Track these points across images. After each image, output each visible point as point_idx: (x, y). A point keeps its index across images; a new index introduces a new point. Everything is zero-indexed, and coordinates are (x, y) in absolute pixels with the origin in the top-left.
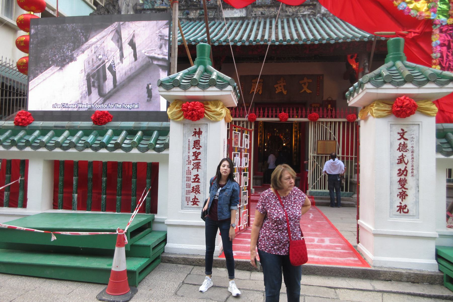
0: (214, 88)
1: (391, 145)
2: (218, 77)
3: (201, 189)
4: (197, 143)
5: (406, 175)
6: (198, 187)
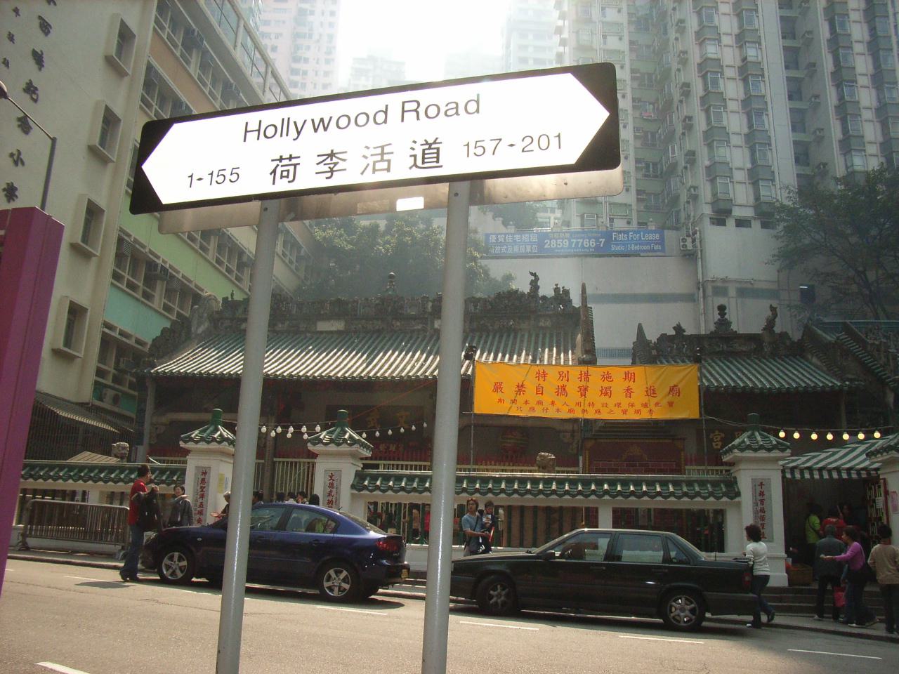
1: (325, 483)
2: (221, 435)
3: (204, 512)
4: (203, 480)
6: (202, 510)
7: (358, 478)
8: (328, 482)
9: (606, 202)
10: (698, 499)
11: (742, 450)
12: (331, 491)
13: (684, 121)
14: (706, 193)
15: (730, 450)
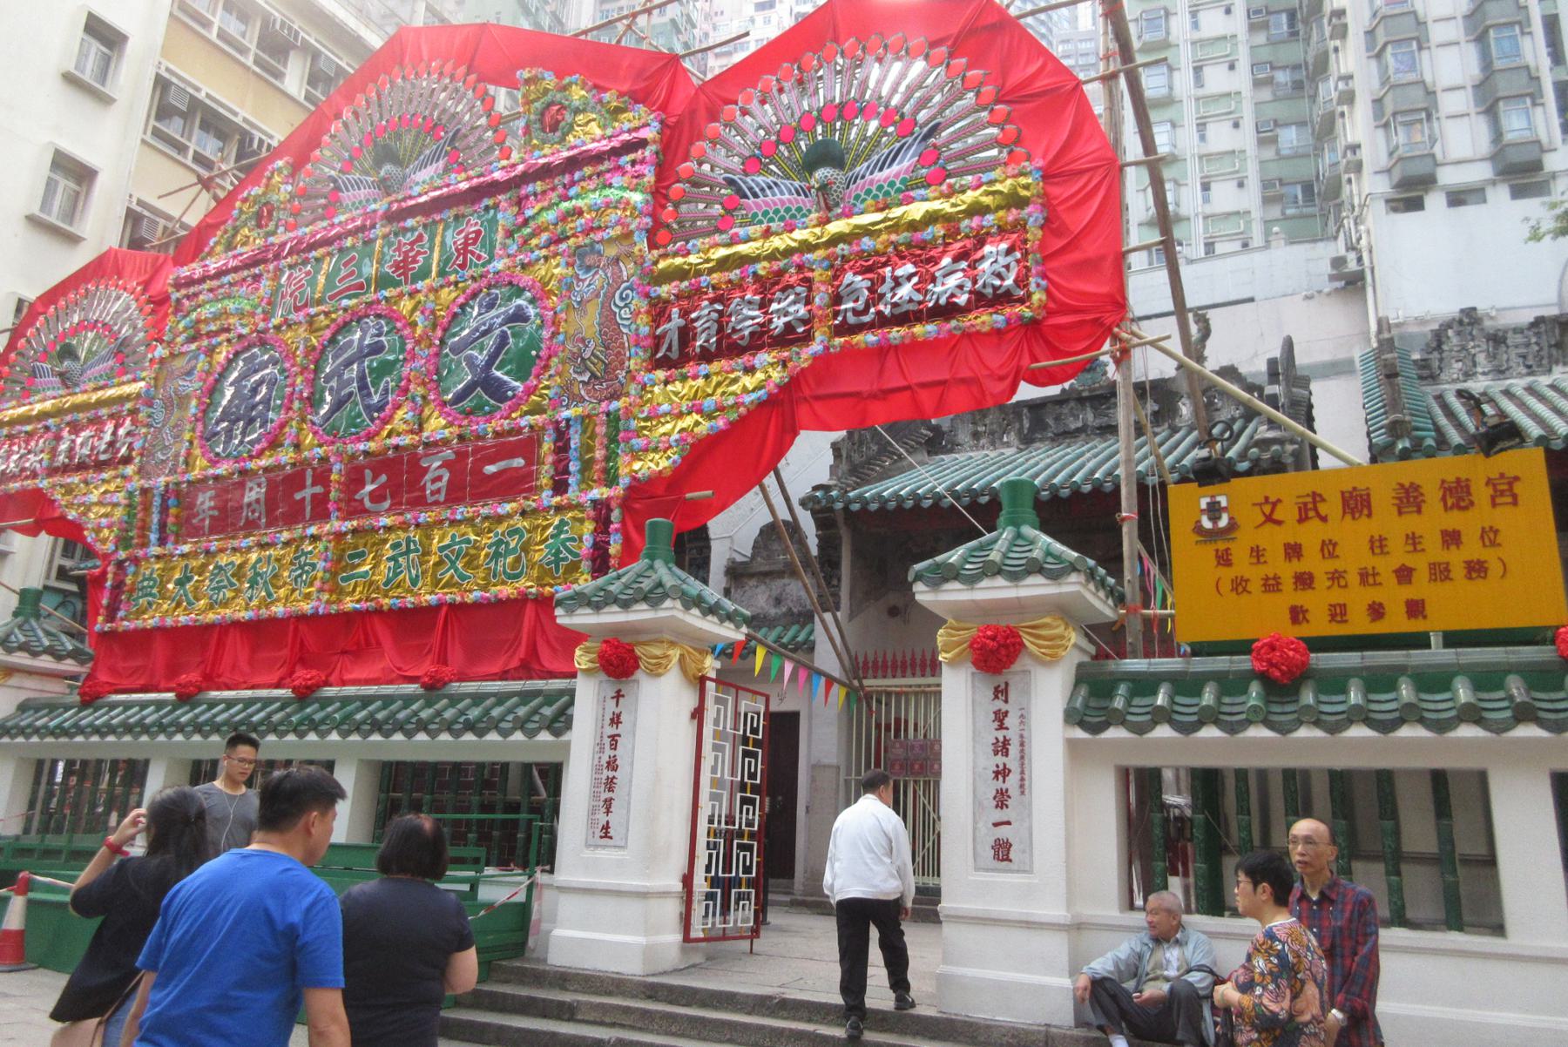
9: (1197, 215)
10: (493, 736)
11: (570, 612)
14: (1374, 151)
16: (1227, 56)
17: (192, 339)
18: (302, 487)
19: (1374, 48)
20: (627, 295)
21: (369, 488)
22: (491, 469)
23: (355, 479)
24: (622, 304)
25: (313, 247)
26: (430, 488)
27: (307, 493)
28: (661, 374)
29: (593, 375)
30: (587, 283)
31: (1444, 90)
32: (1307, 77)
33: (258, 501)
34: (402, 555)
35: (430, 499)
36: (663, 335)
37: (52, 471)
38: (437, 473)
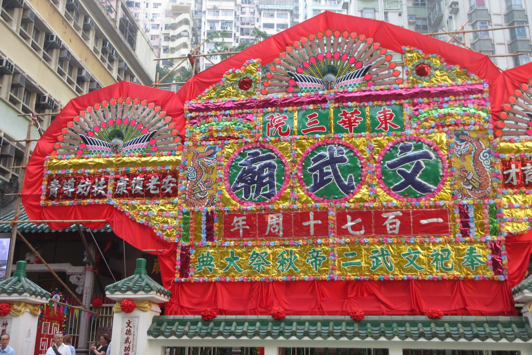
0: (16, 295)
1: (122, 331)
5: (129, 351)
7: (155, 324)
8: (126, 329)
10: (490, 340)
12: (128, 338)
13: (451, 6)
15: (520, 290)
16: (398, 9)
17: (206, 139)
18: (309, 220)
19: (472, 21)
20: (486, 156)
21: (350, 224)
22: (424, 222)
23: (341, 218)
24: (484, 159)
25: (288, 105)
26: (389, 227)
27: (312, 222)
28: (510, 191)
29: (474, 187)
30: (462, 147)
31: (497, 44)
32: (430, 24)
33: (278, 224)
34: (380, 256)
35: (389, 232)
36: (508, 175)
37: (116, 196)
38: (394, 221)
